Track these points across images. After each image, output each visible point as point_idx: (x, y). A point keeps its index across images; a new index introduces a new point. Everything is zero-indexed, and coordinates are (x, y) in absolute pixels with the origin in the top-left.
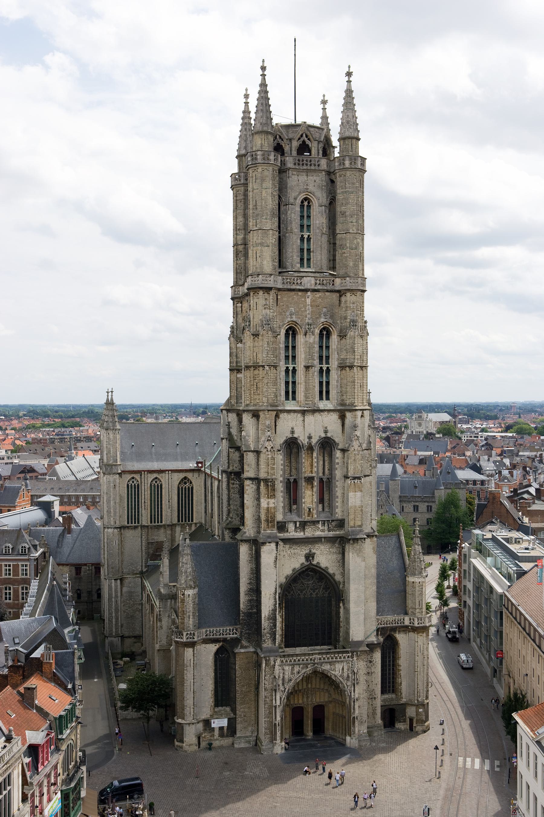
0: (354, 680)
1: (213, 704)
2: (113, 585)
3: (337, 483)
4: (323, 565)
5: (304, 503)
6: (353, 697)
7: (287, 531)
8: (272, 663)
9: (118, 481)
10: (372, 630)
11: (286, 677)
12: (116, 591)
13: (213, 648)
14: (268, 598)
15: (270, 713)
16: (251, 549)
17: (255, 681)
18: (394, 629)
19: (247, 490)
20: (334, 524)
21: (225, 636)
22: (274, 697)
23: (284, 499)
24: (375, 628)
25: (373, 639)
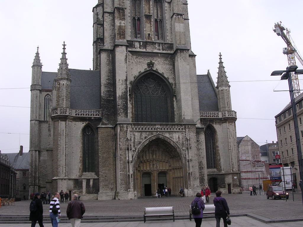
0: (188, 145)
1: (81, 168)
2: (34, 154)
3: (167, 21)
4: (161, 70)
5: (145, 31)
6: (187, 158)
7: (134, 47)
8: (125, 129)
9: (38, 94)
10: (198, 119)
11: (136, 140)
12: (36, 158)
13: (81, 125)
14: (121, 83)
15: (125, 168)
16: (109, 56)
17: (113, 149)
18: (212, 120)
19: (106, 19)
20: (166, 46)
21: (90, 116)
22: (127, 155)
23: (131, 27)
24: (199, 118)
25: (199, 125)
